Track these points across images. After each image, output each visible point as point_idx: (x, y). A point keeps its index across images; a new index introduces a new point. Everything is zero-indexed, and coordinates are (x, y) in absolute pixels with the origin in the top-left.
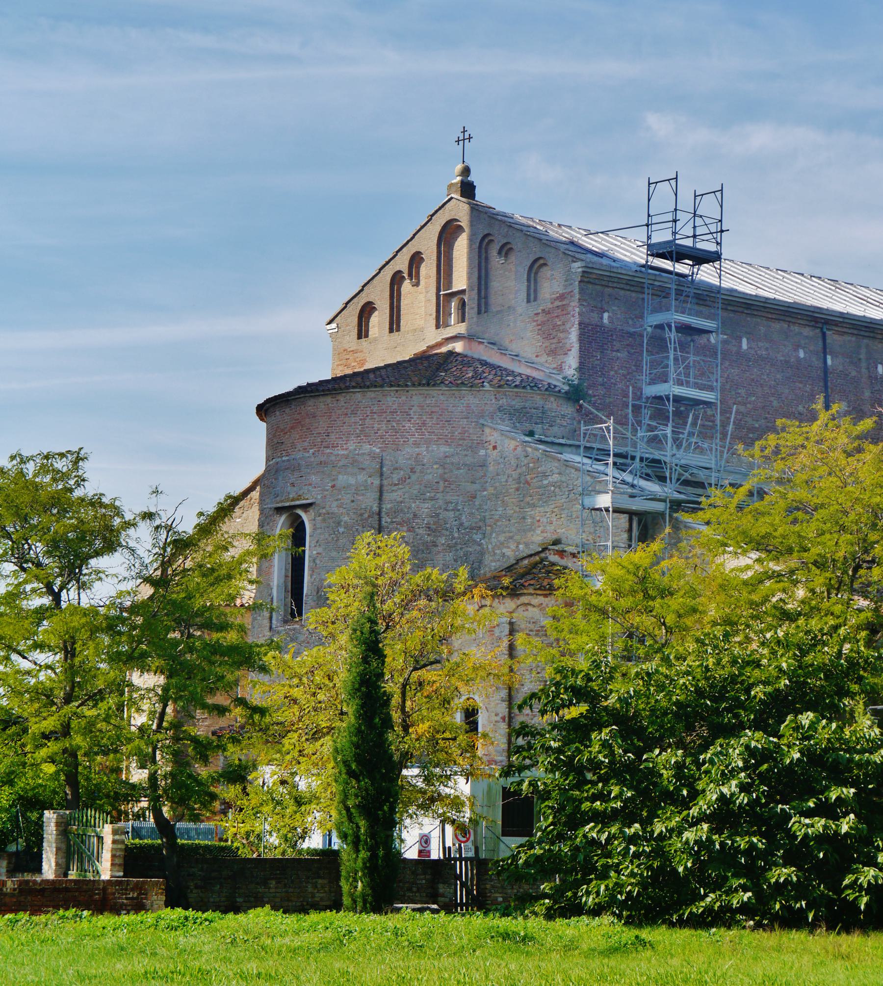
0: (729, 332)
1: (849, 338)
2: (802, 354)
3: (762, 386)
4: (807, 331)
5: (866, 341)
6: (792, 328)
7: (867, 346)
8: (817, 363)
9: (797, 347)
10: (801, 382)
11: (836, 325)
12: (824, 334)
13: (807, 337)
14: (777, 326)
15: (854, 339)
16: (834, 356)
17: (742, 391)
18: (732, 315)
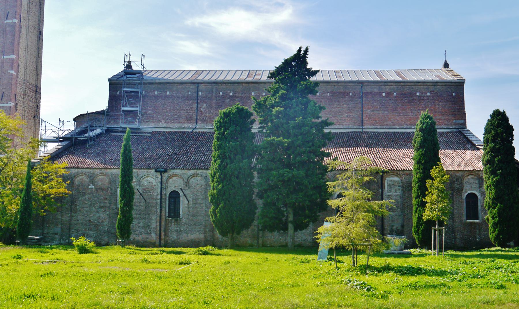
0: (162, 91)
1: (209, 86)
2: (190, 93)
3: (173, 104)
4: (192, 87)
5: (215, 86)
6: (186, 86)
7: (216, 88)
8: (195, 95)
9: (188, 91)
10: (188, 101)
11: (202, 83)
12: (198, 87)
13: (192, 88)
14: (181, 87)
15: (211, 86)
16: (201, 91)
17: (165, 106)
18: (163, 86)
